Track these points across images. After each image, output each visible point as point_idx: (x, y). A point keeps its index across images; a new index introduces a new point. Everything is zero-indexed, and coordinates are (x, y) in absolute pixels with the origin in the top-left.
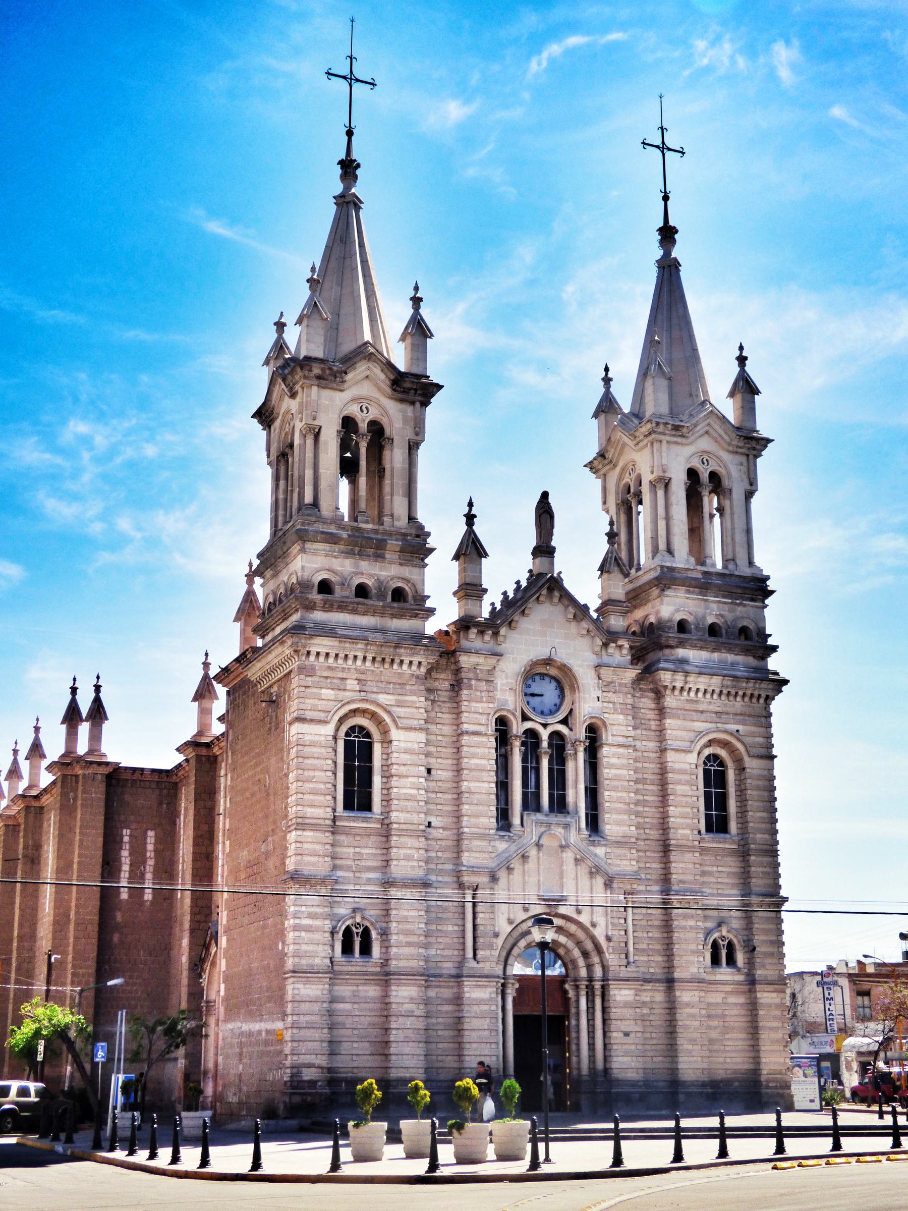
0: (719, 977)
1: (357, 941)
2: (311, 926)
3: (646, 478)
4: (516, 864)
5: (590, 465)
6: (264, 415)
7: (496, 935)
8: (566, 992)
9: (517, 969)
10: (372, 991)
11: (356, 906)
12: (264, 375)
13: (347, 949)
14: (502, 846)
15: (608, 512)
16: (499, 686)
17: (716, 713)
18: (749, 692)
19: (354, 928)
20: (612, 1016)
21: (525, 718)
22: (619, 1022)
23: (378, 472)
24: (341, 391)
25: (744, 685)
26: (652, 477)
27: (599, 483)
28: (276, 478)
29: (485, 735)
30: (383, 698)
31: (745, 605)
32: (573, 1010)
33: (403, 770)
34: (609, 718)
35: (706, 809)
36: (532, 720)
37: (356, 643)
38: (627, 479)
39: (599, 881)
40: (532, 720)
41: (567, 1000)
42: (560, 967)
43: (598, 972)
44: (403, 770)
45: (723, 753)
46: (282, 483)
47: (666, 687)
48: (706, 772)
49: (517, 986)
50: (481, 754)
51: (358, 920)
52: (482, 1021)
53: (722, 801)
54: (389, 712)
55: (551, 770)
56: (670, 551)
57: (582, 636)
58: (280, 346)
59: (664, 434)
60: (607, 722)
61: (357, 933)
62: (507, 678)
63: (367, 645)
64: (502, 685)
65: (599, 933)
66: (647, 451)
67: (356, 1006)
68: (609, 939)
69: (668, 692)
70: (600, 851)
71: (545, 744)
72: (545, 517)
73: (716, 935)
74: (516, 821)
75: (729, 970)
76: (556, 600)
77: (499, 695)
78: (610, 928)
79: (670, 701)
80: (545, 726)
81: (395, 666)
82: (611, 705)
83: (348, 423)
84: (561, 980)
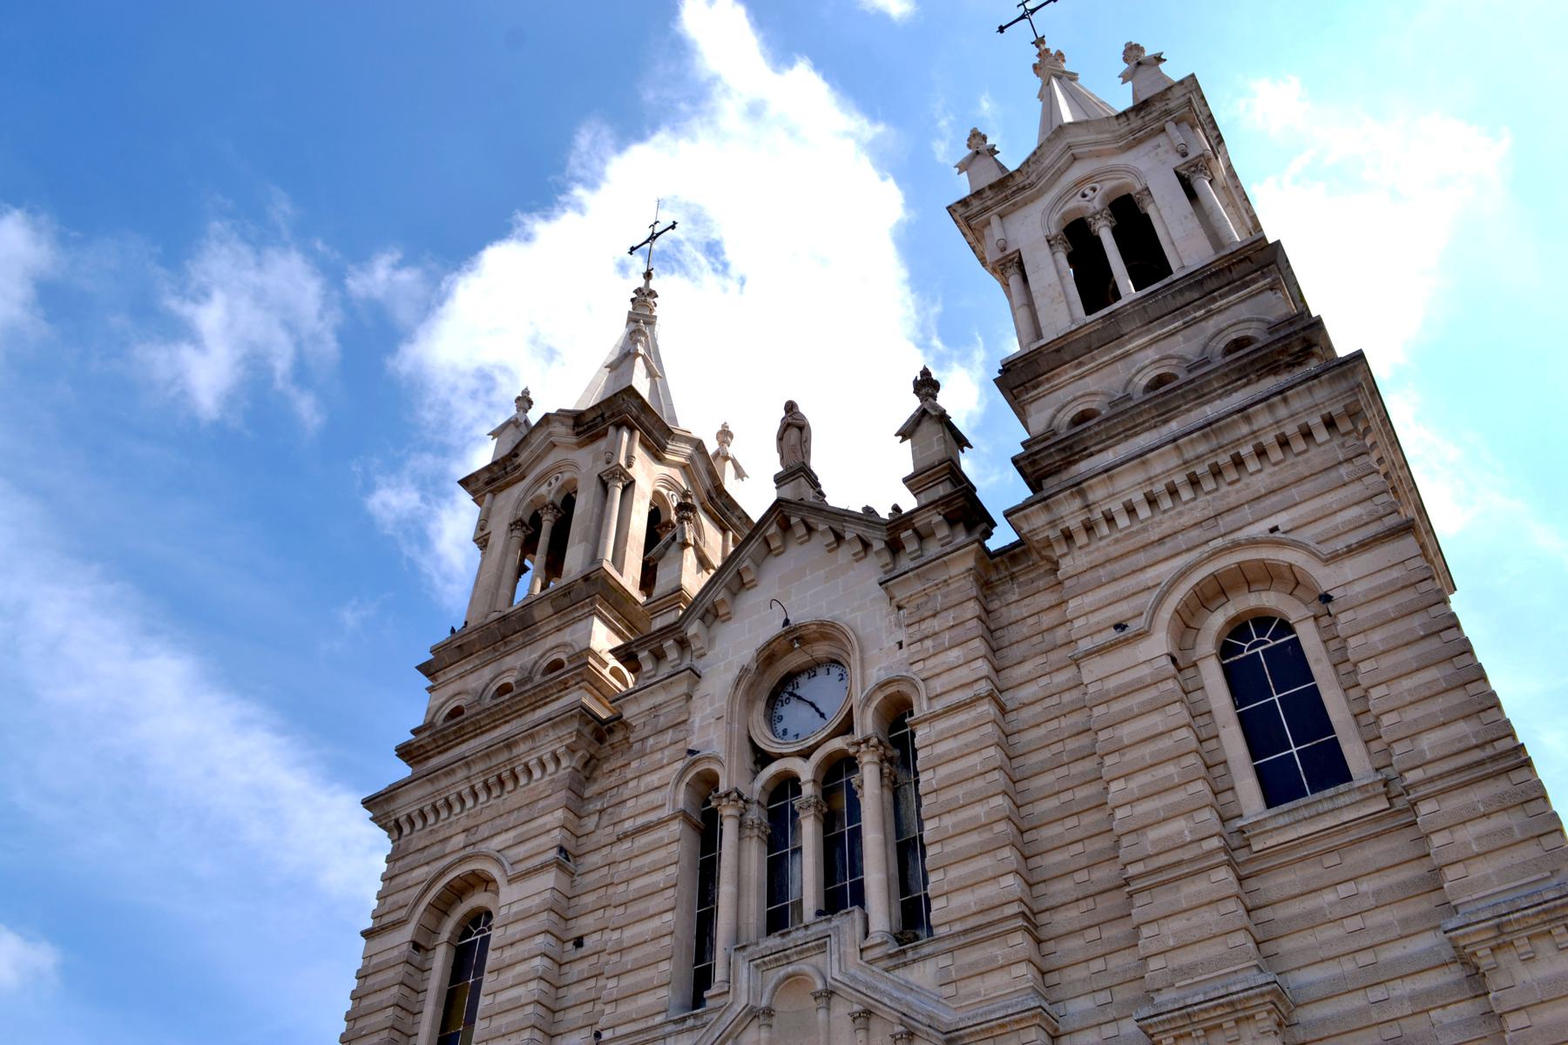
16: (697, 724)
17: (1198, 524)
18: (1269, 439)
25: (1245, 429)
29: (661, 823)
35: (1255, 751)
36: (782, 756)
37: (453, 771)
40: (782, 756)
57: (858, 558)
59: (987, 209)
63: (467, 765)
64: (703, 719)
72: (793, 434)
76: (801, 531)
80: (805, 754)
81: (523, 780)
82: (929, 643)
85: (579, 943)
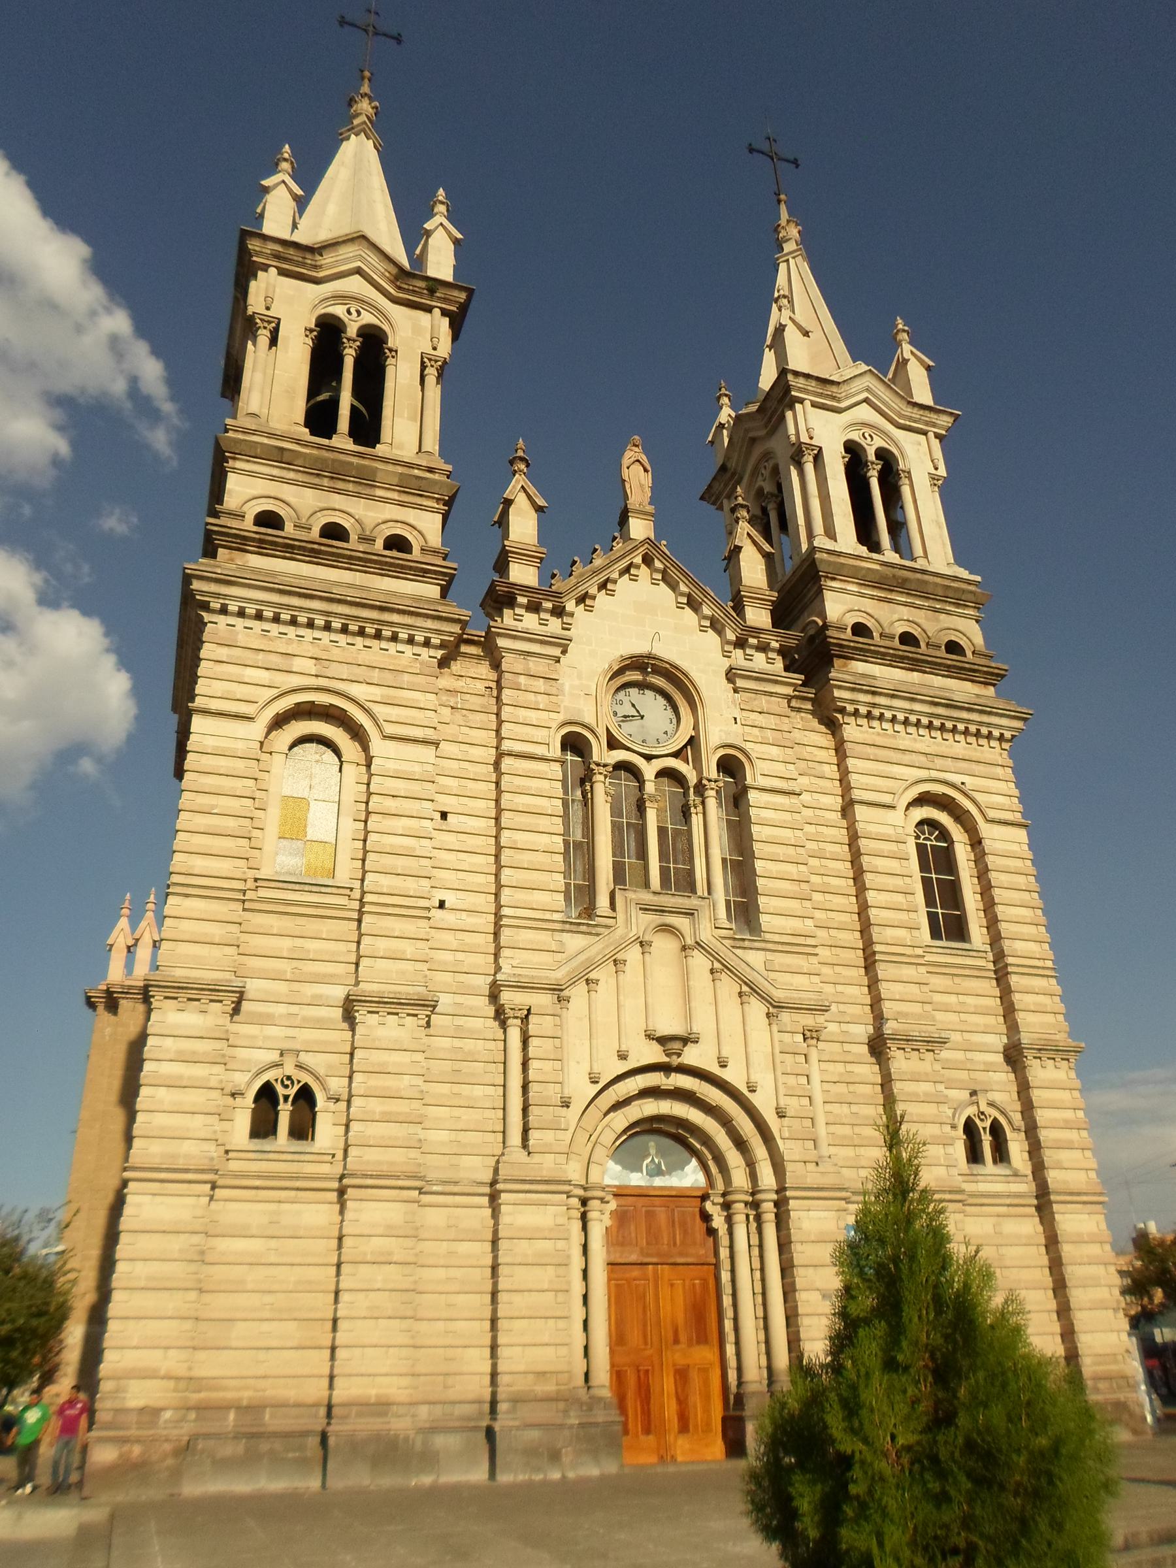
0: (983, 1187)
1: (285, 1112)
2: (181, 1077)
4: (604, 974)
7: (566, 1104)
8: (706, 1217)
9: (612, 1174)
10: (318, 1213)
11: (286, 1045)
13: (263, 1127)
14: (574, 942)
16: (567, 688)
19: (279, 1088)
20: (798, 1259)
22: (811, 1270)
24: (317, 281)
30: (355, 690)
31: (948, 613)
33: (390, 804)
36: (628, 749)
39: (757, 1009)
40: (628, 749)
42: (694, 1172)
43: (767, 1178)
44: (390, 804)
45: (943, 818)
48: (921, 849)
49: (613, 1205)
51: (289, 1069)
52: (538, 1271)
53: (951, 894)
54: (367, 711)
55: (662, 831)
56: (830, 533)
60: (753, 755)
61: (286, 1098)
62: (580, 677)
65: (763, 1102)
67: (273, 1243)
68: (781, 1114)
70: (756, 958)
73: (971, 1111)
74: (603, 901)
75: (1001, 1170)
77: (566, 702)
78: (782, 1091)
79: (852, 730)
80: (649, 758)
85: (444, 815)
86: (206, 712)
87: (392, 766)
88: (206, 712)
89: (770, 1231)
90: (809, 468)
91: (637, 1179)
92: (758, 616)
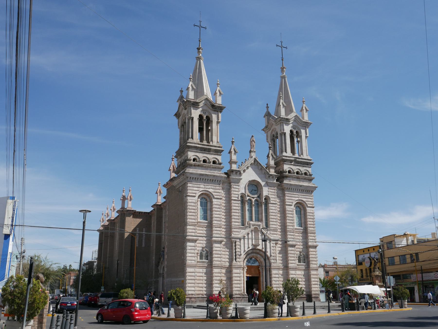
3: (279, 133)
5: (263, 130)
6: (177, 115)
8: (259, 270)
12: (178, 104)
15: (268, 142)
21: (248, 196)
23: (208, 131)
26: (280, 132)
27: (265, 135)
28: (181, 132)
30: (210, 190)
32: (261, 275)
34: (270, 196)
38: (273, 133)
41: (259, 272)
46: (182, 133)
47: (285, 188)
48: (296, 211)
50: (236, 206)
58: (182, 97)
66: (279, 125)
69: (286, 189)
71: (253, 203)
76: (256, 164)
80: (253, 198)
83: (201, 117)
84: (258, 267)
86: (189, 196)
87: (216, 203)
88: (189, 196)
89: (268, 272)
90: (283, 137)
91: (250, 264)
92: (272, 172)
